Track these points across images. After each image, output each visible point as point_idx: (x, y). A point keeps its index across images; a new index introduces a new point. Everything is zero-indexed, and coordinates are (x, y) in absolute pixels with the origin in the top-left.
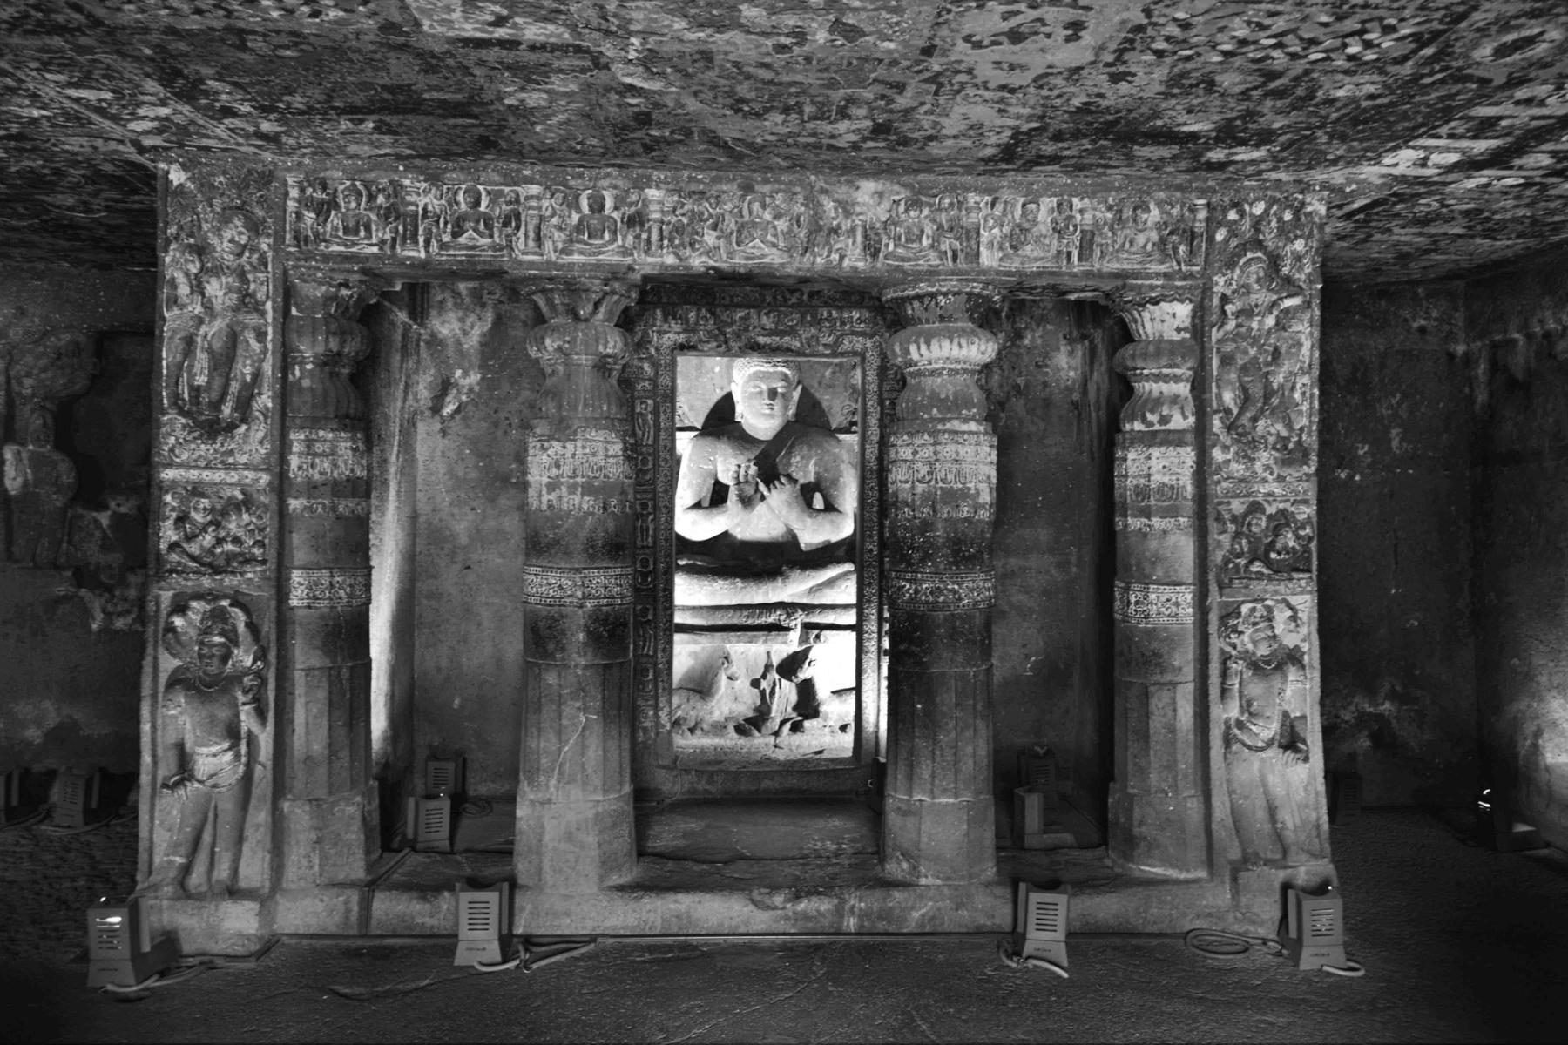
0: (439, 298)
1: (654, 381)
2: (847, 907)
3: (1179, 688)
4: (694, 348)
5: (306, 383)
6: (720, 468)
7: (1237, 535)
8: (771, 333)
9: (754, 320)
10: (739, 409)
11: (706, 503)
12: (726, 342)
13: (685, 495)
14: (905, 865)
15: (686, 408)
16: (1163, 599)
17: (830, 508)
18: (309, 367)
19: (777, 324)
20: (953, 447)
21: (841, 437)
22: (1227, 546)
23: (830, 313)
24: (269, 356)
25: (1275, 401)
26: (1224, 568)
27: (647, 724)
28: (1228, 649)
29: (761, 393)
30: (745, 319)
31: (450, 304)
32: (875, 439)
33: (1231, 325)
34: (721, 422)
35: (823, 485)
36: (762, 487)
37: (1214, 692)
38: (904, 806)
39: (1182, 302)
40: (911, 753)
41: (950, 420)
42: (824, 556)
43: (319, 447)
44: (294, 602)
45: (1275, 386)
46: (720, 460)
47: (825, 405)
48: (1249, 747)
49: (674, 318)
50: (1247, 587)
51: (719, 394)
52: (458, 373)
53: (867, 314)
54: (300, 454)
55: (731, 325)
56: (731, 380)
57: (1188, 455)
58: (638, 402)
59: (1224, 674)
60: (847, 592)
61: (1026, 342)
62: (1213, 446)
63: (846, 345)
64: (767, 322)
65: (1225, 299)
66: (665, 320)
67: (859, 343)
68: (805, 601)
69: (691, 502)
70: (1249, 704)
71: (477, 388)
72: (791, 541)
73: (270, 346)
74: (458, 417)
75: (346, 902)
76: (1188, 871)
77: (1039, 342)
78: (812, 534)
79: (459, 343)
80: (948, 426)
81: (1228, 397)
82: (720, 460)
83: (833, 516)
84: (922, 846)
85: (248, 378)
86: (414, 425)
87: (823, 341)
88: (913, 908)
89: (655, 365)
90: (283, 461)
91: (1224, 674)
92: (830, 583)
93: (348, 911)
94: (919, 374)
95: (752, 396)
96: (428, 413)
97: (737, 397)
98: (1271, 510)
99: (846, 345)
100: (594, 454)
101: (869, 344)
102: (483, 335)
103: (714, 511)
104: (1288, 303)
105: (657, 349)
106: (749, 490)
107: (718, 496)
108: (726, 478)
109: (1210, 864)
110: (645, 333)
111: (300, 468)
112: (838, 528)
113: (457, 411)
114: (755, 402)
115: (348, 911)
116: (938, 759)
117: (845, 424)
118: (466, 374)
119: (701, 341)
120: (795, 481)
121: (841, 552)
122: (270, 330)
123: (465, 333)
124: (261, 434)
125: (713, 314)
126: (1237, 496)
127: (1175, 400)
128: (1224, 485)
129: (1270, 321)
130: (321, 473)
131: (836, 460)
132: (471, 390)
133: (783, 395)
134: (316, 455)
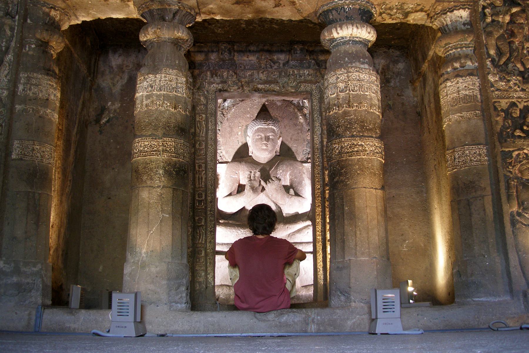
0: (102, 69)
1: (206, 105)
2: (310, 319)
3: (486, 198)
4: (226, 91)
5: (31, 53)
6: (241, 177)
7: (505, 119)
8: (265, 82)
9: (256, 76)
10: (250, 150)
12: (242, 86)
14: (342, 298)
15: (224, 153)
16: (472, 153)
18: (33, 46)
19: (267, 77)
20: (357, 74)
21: (304, 164)
22: (502, 124)
23: (293, 72)
24: (14, 39)
25: (516, 54)
26: (501, 134)
27: (201, 280)
28: (509, 174)
29: (261, 138)
30: (251, 75)
31: (107, 72)
32: (319, 132)
33: (489, 20)
35: (294, 185)
36: (263, 183)
37: (504, 198)
38: (340, 265)
39: (464, 9)
40: (343, 234)
41: (354, 62)
43: (34, 81)
44: (14, 156)
45: (514, 48)
46: (241, 173)
47: (294, 149)
48: (525, 225)
49: (216, 76)
50: (514, 142)
52: (110, 103)
53: (312, 72)
54: (24, 84)
55: (245, 78)
57: (476, 81)
58: (197, 116)
59: (508, 187)
60: (307, 236)
61: (392, 84)
62: (488, 74)
63: (302, 88)
64: (263, 76)
65: (484, 8)
66: (212, 77)
67: (309, 87)
70: (523, 203)
71: (118, 111)
73: (15, 35)
74: (108, 124)
75: (30, 314)
76: (499, 296)
77: (398, 84)
79: (111, 89)
80: (354, 65)
81: (492, 52)
82: (241, 173)
84: (352, 285)
85: (4, 49)
86: (86, 127)
87: (291, 85)
88: (348, 319)
89: (206, 98)
90: (15, 86)
91: (508, 187)
92: (299, 231)
93: (30, 319)
94: (338, 45)
95: (257, 140)
96: (93, 123)
97: (250, 144)
98: (521, 106)
99: (302, 88)
100: (171, 81)
101: (314, 87)
102: (123, 86)
103: (238, 195)
104: (514, 10)
105: (207, 91)
107: (241, 189)
109: (511, 292)
110: (202, 84)
111: (23, 90)
113: (108, 121)
114: (259, 143)
115: (30, 319)
116: (358, 235)
117: (305, 159)
118: (113, 104)
119: (229, 86)
122: (16, 28)
123: (114, 85)
124: (6, 72)
125: (236, 73)
126: (504, 98)
127: (467, 56)
128: (496, 92)
129: (507, 18)
130: (33, 93)
132: (115, 111)
133: (273, 140)
134: (32, 84)
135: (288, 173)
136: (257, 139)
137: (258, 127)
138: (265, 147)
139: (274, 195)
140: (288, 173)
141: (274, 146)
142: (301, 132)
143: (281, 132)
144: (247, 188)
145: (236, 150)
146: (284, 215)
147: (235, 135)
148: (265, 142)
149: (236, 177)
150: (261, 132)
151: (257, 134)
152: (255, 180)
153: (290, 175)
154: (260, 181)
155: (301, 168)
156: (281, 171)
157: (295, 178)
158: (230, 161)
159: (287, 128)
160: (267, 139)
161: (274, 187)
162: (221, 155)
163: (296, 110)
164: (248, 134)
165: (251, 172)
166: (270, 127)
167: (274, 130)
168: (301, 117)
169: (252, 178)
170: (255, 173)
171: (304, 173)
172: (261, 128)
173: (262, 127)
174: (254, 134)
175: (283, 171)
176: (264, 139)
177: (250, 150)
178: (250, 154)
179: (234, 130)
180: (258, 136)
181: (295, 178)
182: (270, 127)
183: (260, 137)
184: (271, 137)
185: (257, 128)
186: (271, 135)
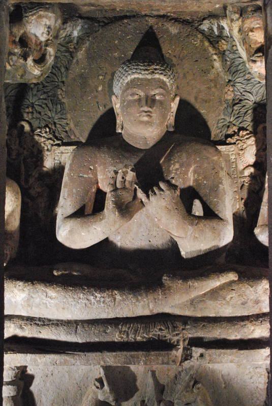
11: (89, 210)
13: (65, 205)
15: (72, 125)
17: (210, 214)
21: (219, 147)
29: (139, 100)
34: (105, 135)
36: (141, 194)
42: (206, 264)
51: (102, 110)
56: (111, 93)
68: (187, 313)
69: (70, 211)
72: (173, 248)
78: (193, 242)
83: (214, 223)
92: (214, 294)
108: (106, 187)
112: (217, 234)
121: (222, 260)
131: (215, 168)
133: (161, 103)
135: (192, 169)
136: (130, 101)
137: (133, 77)
138: (146, 119)
139: (164, 220)
141: (164, 116)
142: (216, 86)
143: (178, 87)
144: (109, 203)
145: (95, 120)
146: (183, 253)
147: (92, 92)
148: (146, 109)
149: (91, 176)
151: (129, 91)
152: (124, 188)
153: (195, 172)
154: (135, 189)
155: (215, 158)
156: (177, 166)
157: (205, 178)
158: (84, 141)
159: (189, 77)
160: (151, 101)
161: (163, 203)
162: (67, 129)
163: (207, 44)
164: (115, 90)
165: (116, 173)
166: (157, 76)
167: (164, 83)
168: (215, 57)
169: (118, 186)
170: (125, 173)
171: (222, 169)
172: (138, 79)
173: (140, 76)
174: (124, 91)
175: (181, 166)
176: (144, 102)
177: (118, 121)
179: (90, 82)
180: (133, 95)
181: (205, 178)
182: (157, 76)
183: (136, 97)
184: (157, 98)
185: (129, 78)
186: (159, 94)
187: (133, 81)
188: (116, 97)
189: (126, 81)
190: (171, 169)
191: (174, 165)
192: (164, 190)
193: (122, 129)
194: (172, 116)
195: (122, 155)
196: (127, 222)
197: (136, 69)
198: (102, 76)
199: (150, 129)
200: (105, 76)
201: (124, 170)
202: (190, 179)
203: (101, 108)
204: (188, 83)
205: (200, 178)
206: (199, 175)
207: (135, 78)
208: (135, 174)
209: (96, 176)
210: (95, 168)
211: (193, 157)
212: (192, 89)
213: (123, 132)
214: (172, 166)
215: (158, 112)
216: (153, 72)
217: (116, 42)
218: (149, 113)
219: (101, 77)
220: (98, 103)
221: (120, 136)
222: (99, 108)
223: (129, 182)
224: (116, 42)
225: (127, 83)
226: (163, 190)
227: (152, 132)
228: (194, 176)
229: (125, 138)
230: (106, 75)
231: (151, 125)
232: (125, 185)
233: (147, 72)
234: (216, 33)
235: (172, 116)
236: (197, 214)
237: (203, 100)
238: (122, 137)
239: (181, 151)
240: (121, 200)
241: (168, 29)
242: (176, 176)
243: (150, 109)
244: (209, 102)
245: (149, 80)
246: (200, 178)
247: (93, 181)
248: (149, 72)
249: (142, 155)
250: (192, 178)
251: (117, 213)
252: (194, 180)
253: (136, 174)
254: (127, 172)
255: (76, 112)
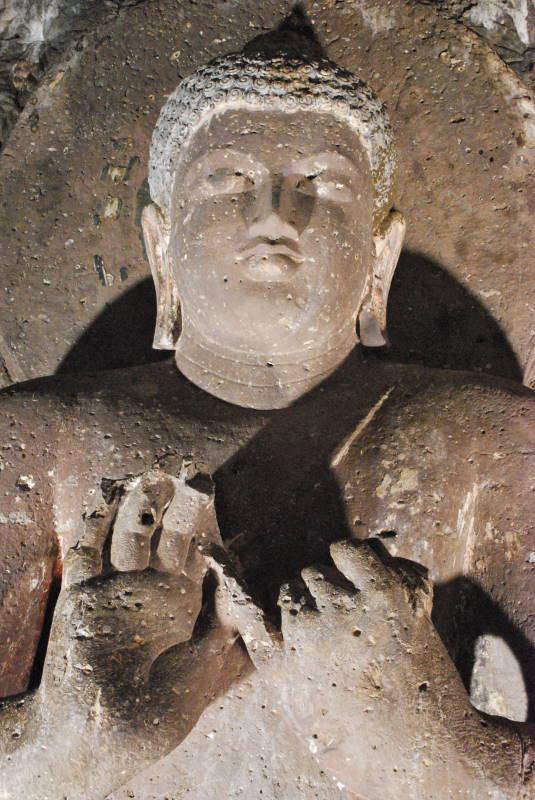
29: (247, 199)
51: (112, 287)
106: (165, 620)
120: (409, 573)
133: (337, 212)
135: (470, 499)
136: (208, 205)
137: (221, 107)
138: (272, 272)
139: (355, 753)
140: (470, 499)
145: (83, 322)
149: (22, 518)
150: (243, 143)
151: (206, 165)
152: (151, 573)
153: (484, 512)
154: (210, 584)
156: (409, 480)
159: (435, 177)
160: (296, 201)
161: (354, 658)
163: (494, 64)
165: (114, 492)
166: (322, 106)
167: (346, 133)
169: (121, 557)
170: (159, 497)
172: (243, 114)
173: (252, 104)
175: (427, 479)
176: (264, 201)
178: (163, 341)
179: (77, 189)
182: (322, 106)
183: (233, 186)
184: (323, 190)
185: (207, 114)
186: (331, 176)
187: (219, 124)
188: (158, 209)
189: (195, 129)
190: (381, 492)
191: (397, 477)
192: (359, 585)
193: (176, 332)
194: (380, 291)
195: (165, 430)
196: (172, 747)
197: (236, 77)
198: (121, 167)
199: (289, 322)
200: (129, 169)
201: (156, 477)
202: (464, 542)
203: (108, 277)
204: (429, 195)
205: (509, 537)
206: (501, 528)
207: (230, 112)
208: (209, 501)
209: (46, 518)
210: (45, 484)
211: (475, 445)
212: (447, 217)
213: (177, 348)
214: (387, 480)
215: (325, 250)
216: (306, 91)
217: (176, 55)
218: (283, 250)
219: (115, 173)
220: (98, 259)
221: (169, 362)
222: (101, 276)
223: (179, 539)
224: (176, 55)
225: (200, 135)
226: (350, 588)
227: (300, 336)
228: (479, 530)
229: (187, 367)
230: (135, 167)
231: (293, 302)
232: (155, 558)
233: (278, 89)
234: (525, 39)
235: (380, 291)
236: (495, 706)
237: (488, 254)
238: (174, 367)
239: (423, 421)
240: (130, 634)
241: (357, 14)
242: (404, 528)
243: (290, 232)
244: (511, 261)
245: (287, 119)
246: (509, 537)
247: (32, 539)
248: (290, 87)
249: (251, 431)
250: (470, 541)
251: (98, 708)
252: (476, 549)
253: (217, 504)
254: (170, 491)
255: (17, 289)
